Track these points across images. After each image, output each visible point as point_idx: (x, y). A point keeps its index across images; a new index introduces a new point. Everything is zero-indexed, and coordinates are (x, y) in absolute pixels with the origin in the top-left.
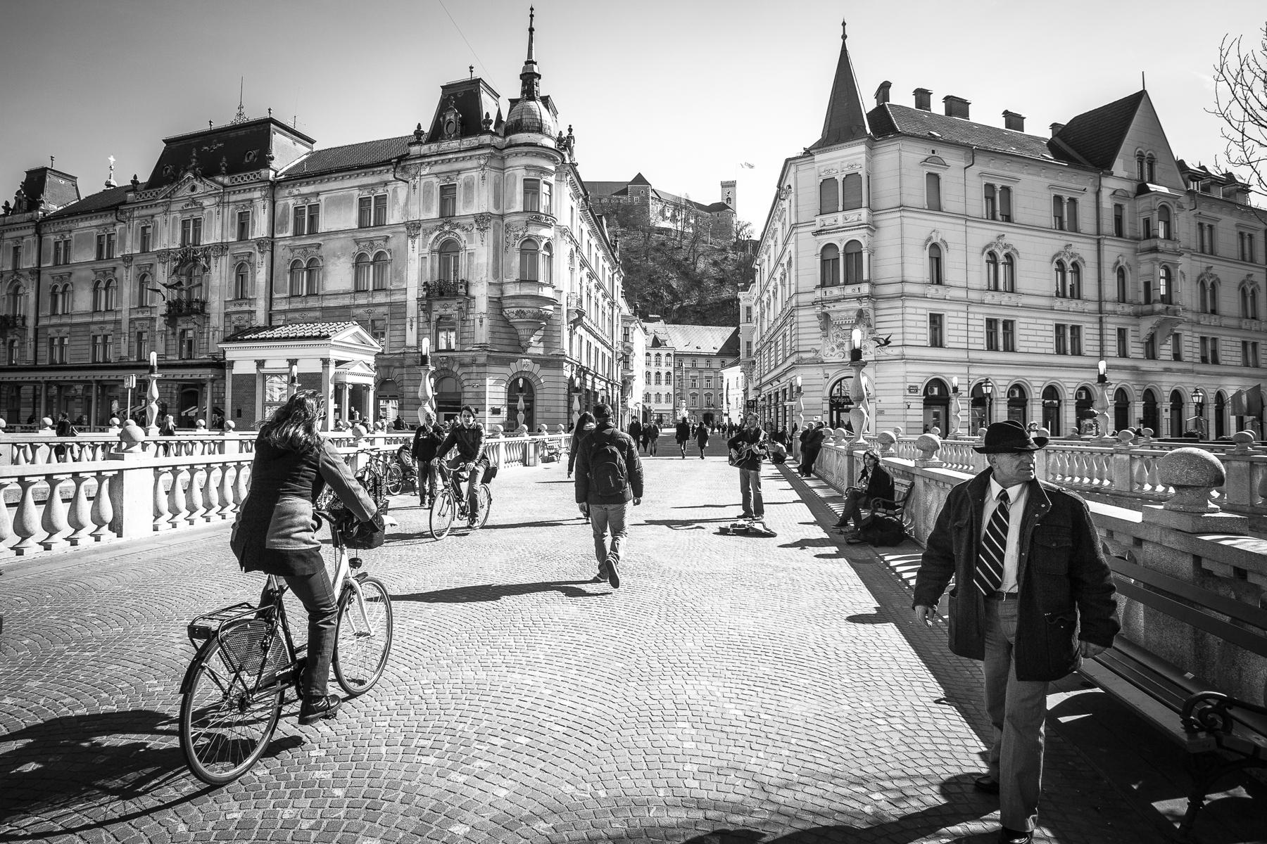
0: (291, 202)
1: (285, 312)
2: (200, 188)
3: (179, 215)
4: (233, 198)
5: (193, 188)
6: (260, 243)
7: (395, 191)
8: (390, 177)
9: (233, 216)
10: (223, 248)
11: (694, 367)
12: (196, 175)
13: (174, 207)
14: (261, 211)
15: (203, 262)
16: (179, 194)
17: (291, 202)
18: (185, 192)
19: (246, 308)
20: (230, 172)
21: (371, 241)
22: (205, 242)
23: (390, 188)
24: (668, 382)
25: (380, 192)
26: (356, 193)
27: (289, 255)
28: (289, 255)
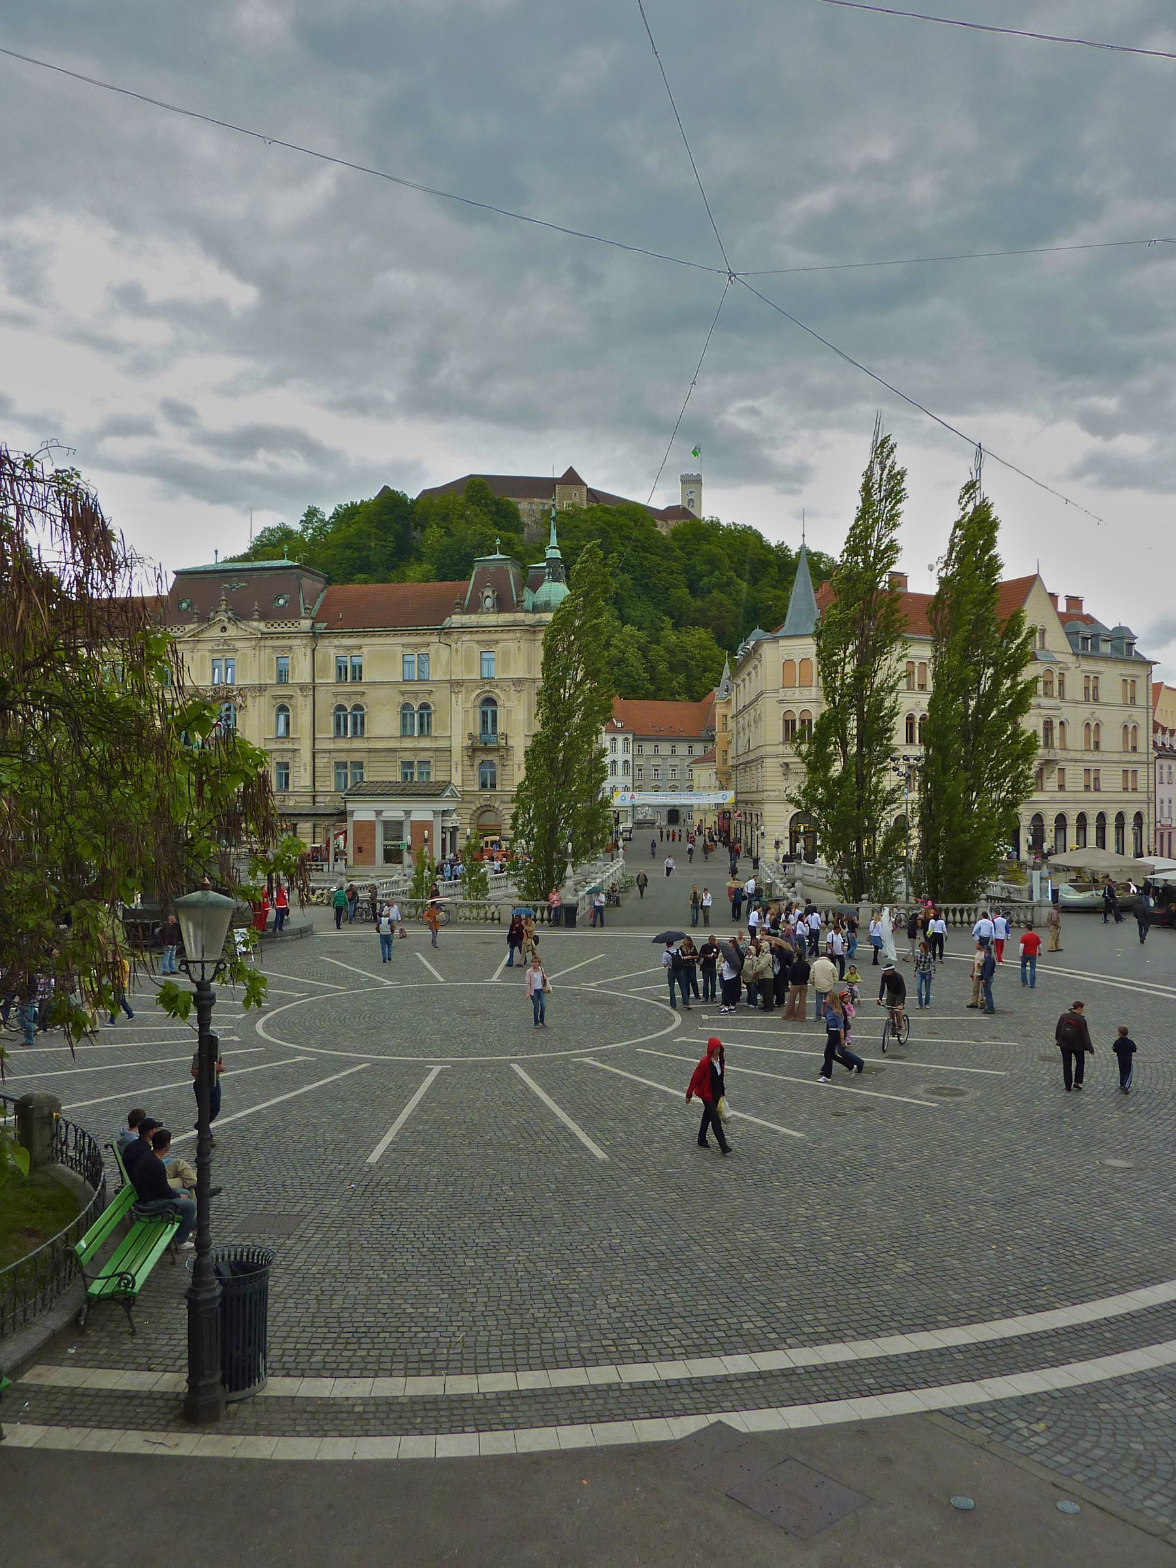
0: (332, 652)
1: (329, 751)
2: (232, 631)
3: (208, 654)
4: (270, 643)
5: (224, 629)
6: (302, 687)
7: (437, 651)
8: (435, 639)
9: (270, 660)
10: (261, 688)
11: (656, 754)
12: (229, 619)
13: (200, 646)
14: (301, 658)
15: (239, 700)
16: (207, 635)
17: (332, 652)
18: (215, 632)
19: (290, 746)
20: (263, 617)
21: (416, 693)
22: (240, 682)
23: (432, 648)
24: (625, 774)
25: (423, 650)
26: (400, 649)
27: (333, 700)
28: (333, 700)
